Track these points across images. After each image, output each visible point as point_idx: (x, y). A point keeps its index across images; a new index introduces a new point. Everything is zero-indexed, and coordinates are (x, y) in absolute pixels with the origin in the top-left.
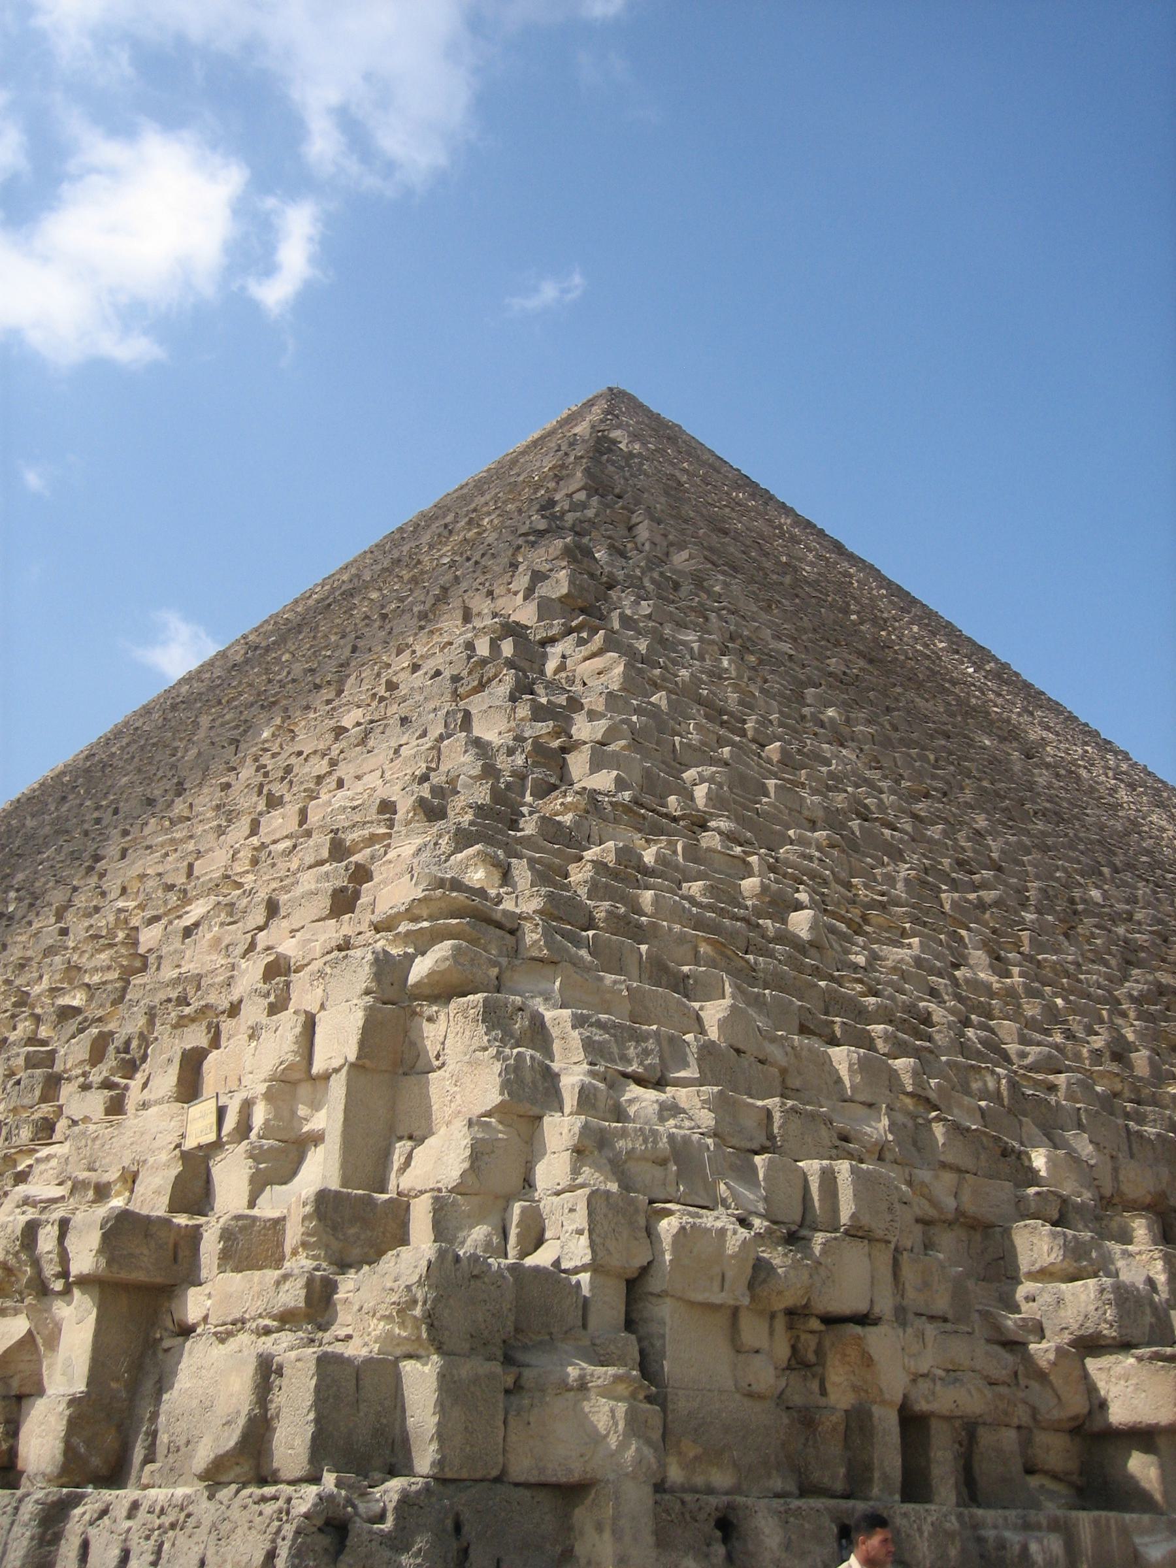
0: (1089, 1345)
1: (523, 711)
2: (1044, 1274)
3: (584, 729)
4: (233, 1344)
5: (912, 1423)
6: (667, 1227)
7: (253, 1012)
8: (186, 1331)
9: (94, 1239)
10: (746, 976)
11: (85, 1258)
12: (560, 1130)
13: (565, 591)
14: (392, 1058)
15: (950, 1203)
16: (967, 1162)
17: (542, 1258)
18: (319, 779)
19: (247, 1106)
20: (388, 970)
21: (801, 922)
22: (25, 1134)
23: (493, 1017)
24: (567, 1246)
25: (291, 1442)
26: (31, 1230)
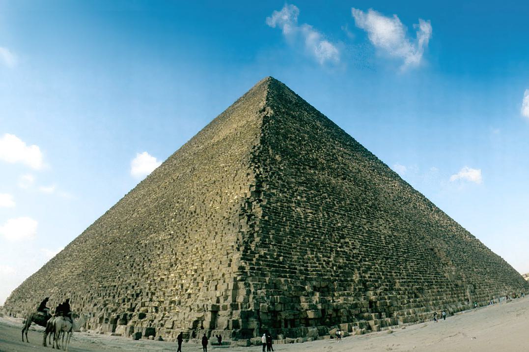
0: (307, 310)
1: (248, 226)
2: (304, 302)
3: (257, 229)
4: (224, 318)
5: (286, 320)
6: (261, 305)
7: (222, 281)
8: (219, 315)
9: (211, 307)
10: (271, 272)
11: (210, 309)
12: (251, 296)
13: (255, 190)
14: (236, 288)
15: (294, 295)
16: (296, 290)
17: (249, 309)
18: (222, 231)
19: (223, 293)
20: (235, 279)
21: (281, 258)
22: (197, 290)
23: (245, 284)
24: (252, 308)
25: (231, 326)
26: (204, 305)
